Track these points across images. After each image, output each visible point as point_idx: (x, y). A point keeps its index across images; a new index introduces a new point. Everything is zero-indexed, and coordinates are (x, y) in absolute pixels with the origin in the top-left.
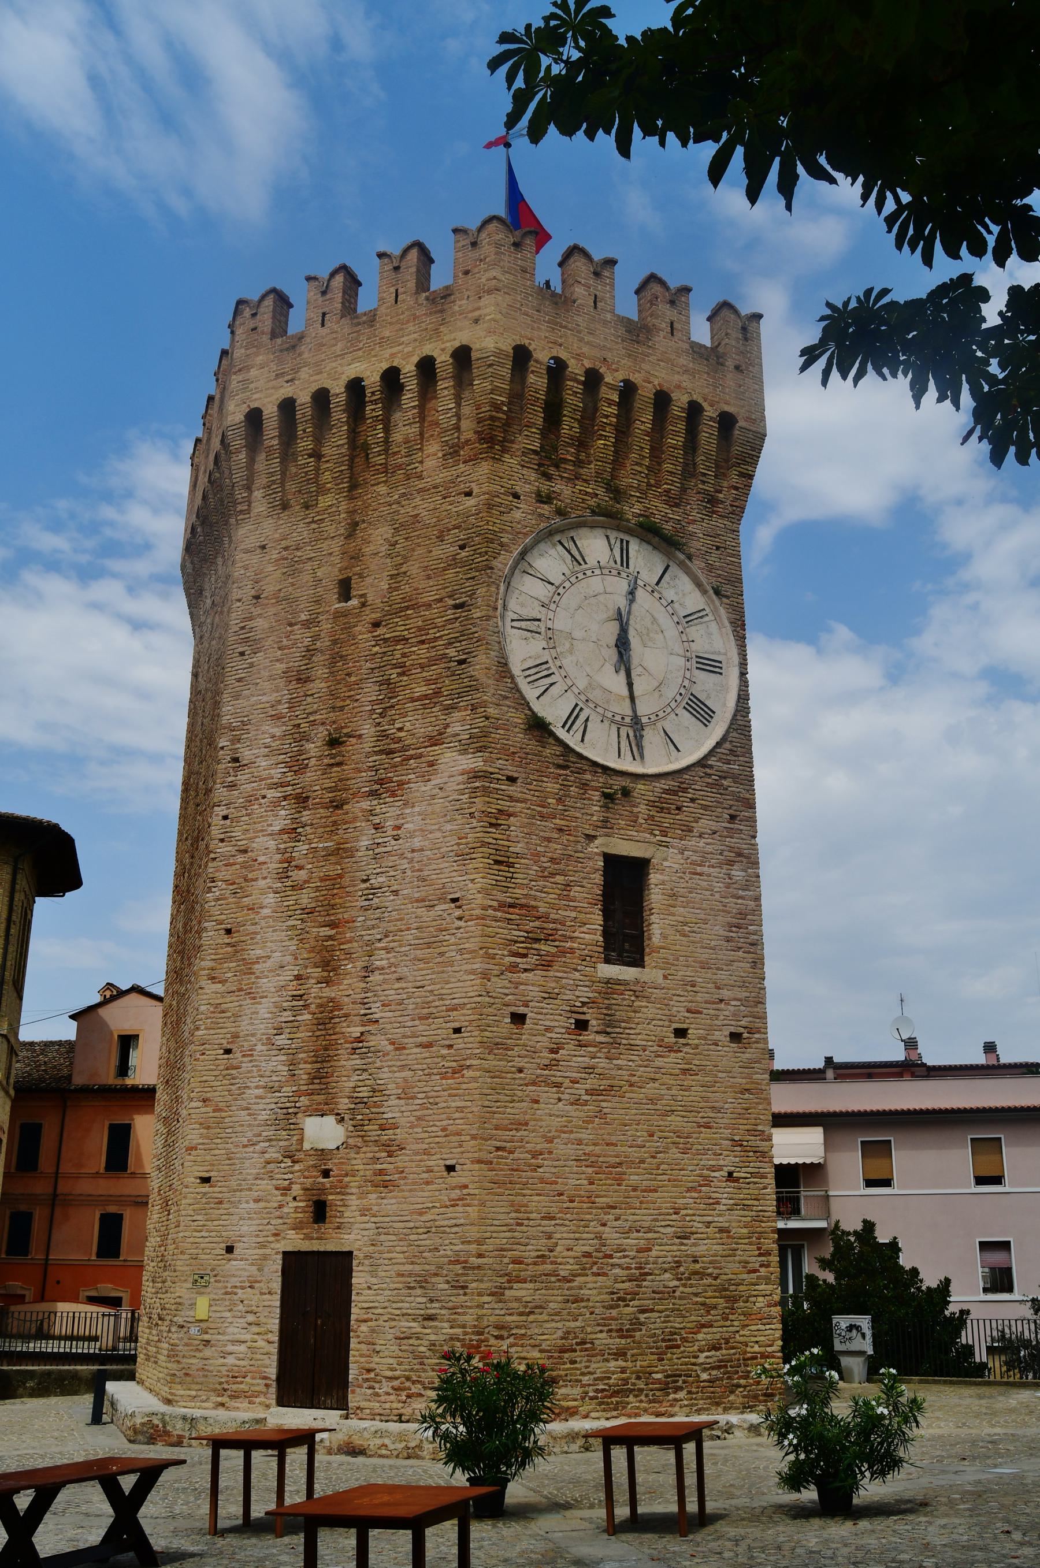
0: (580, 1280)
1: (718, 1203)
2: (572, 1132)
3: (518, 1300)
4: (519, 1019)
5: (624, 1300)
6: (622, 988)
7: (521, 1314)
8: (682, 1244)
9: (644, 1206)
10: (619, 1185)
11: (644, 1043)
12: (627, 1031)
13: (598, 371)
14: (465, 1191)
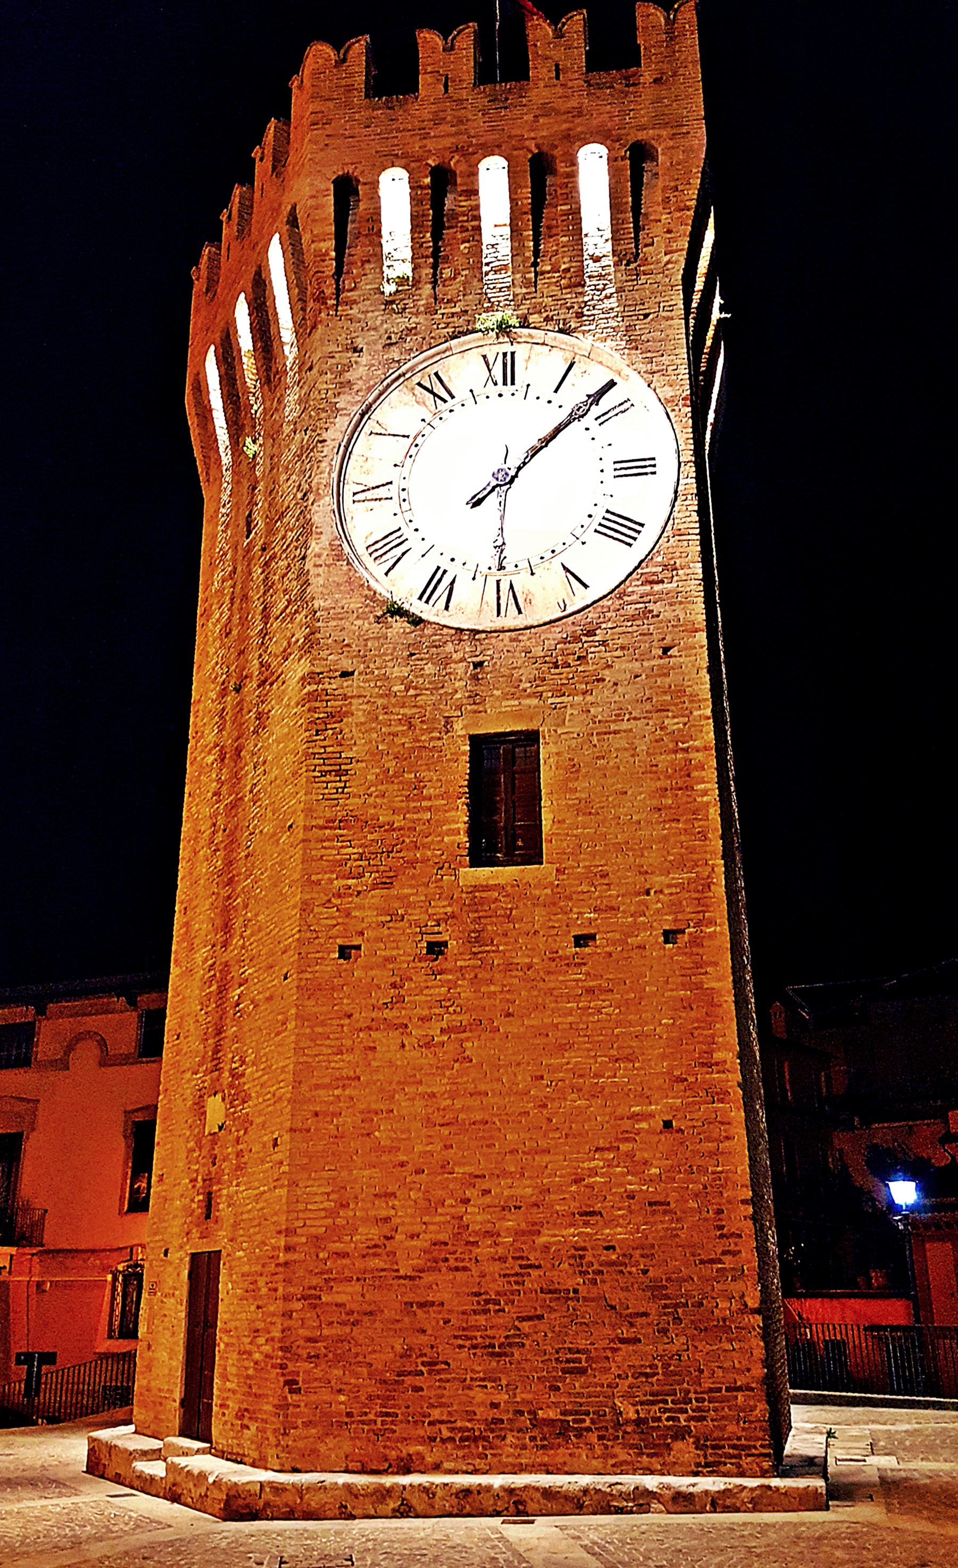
0: (428, 1278)
10: (488, 1146)
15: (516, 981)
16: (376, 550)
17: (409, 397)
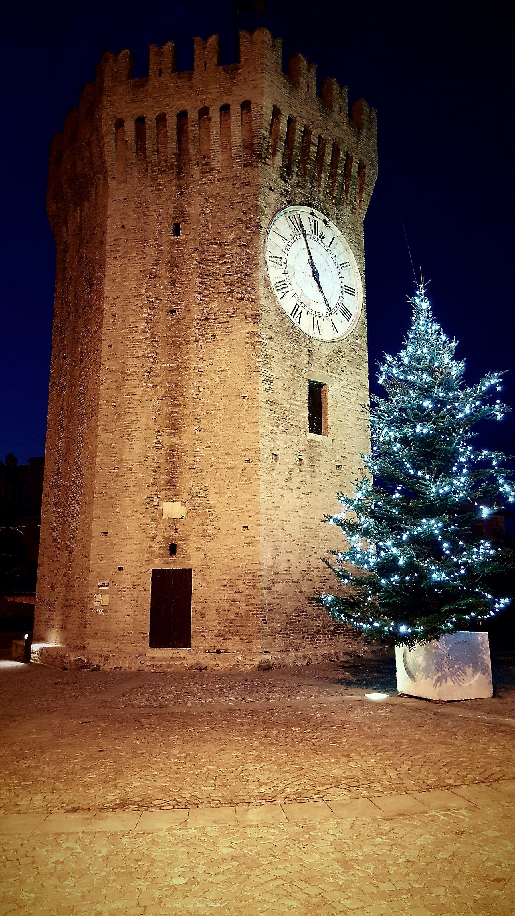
7: (278, 598)
14: (254, 539)
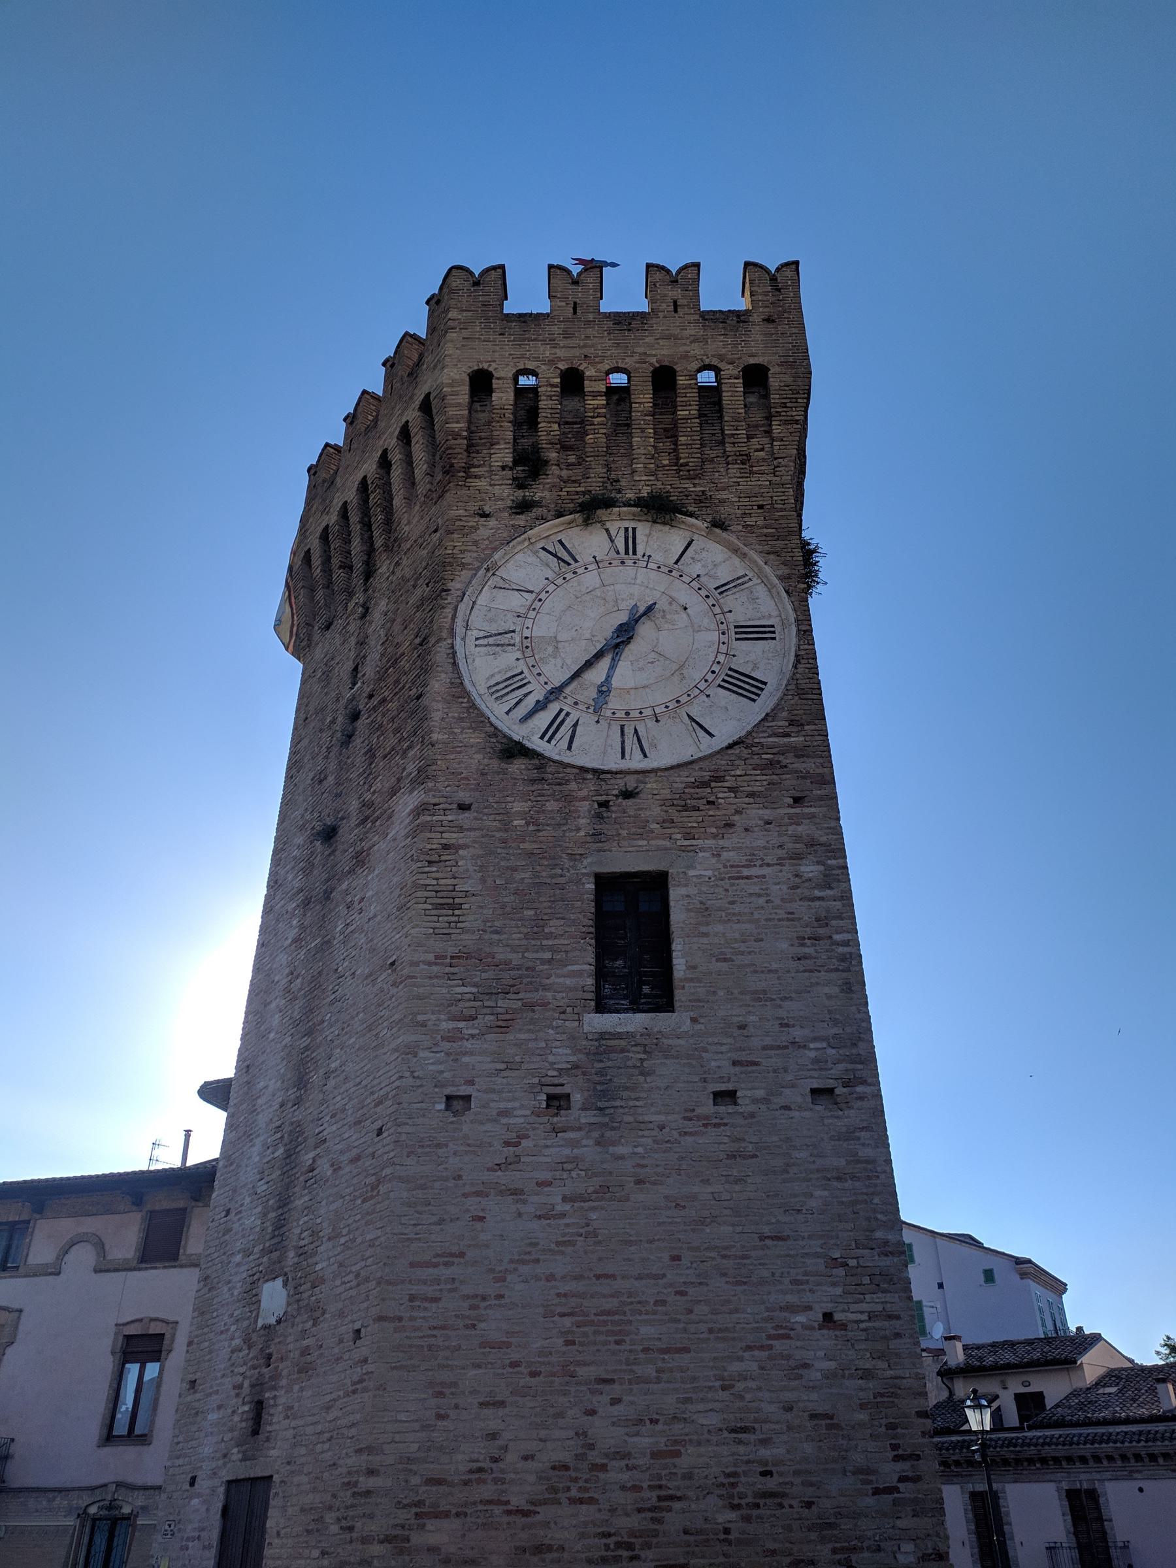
0: (545, 1513)
1: (806, 1366)
2: (537, 1261)
3: (432, 1550)
4: (456, 1103)
5: (630, 1546)
6: (623, 1043)
8: (740, 1442)
9: (665, 1376)
10: (617, 1343)
11: (662, 1118)
12: (631, 1103)
13: (577, 369)
15: (650, 1141)
16: (497, 691)
17: (531, 559)
